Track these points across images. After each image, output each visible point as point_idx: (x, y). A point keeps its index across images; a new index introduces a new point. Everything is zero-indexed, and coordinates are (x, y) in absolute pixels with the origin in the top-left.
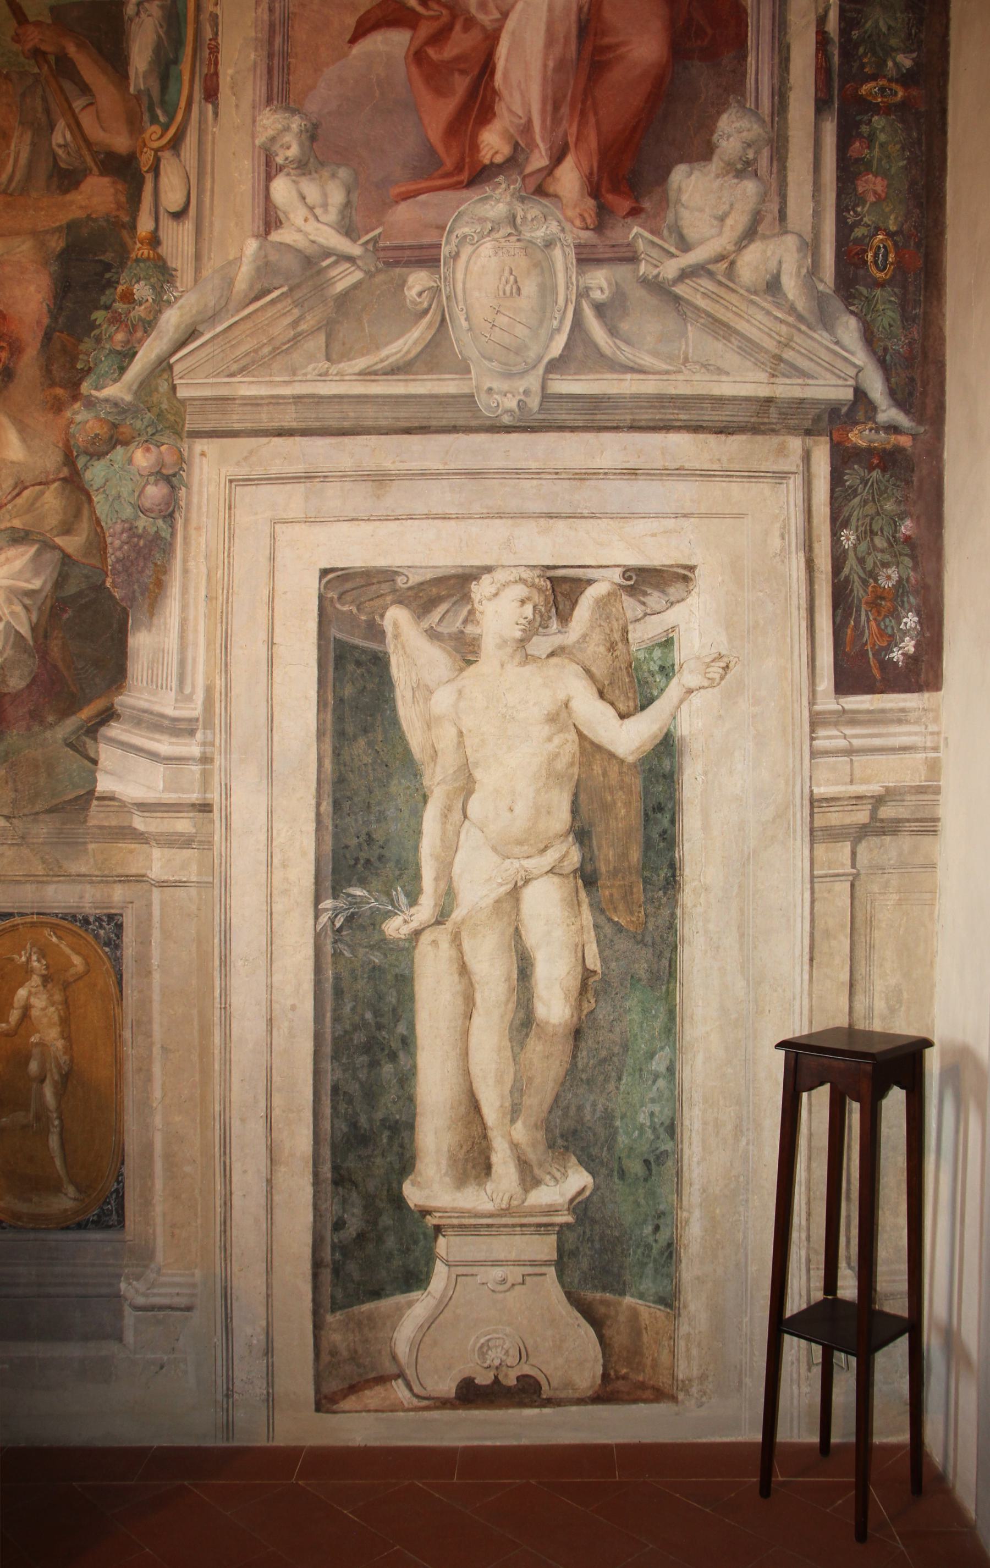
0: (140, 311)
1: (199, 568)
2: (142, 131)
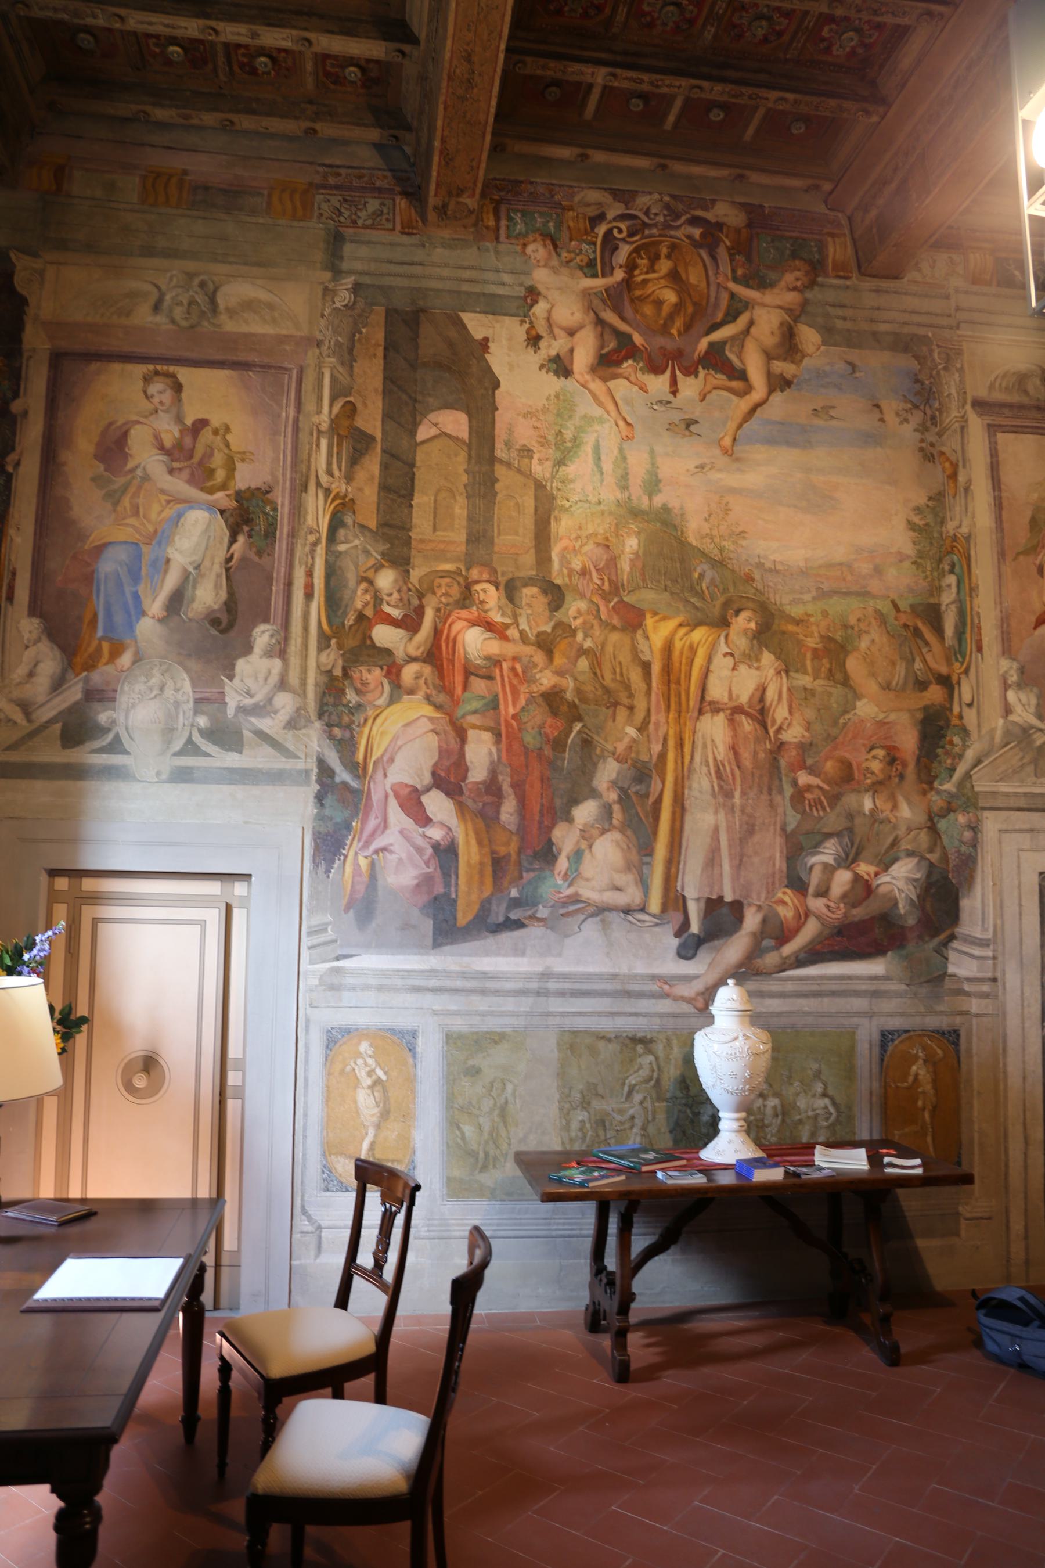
2: (952, 664)
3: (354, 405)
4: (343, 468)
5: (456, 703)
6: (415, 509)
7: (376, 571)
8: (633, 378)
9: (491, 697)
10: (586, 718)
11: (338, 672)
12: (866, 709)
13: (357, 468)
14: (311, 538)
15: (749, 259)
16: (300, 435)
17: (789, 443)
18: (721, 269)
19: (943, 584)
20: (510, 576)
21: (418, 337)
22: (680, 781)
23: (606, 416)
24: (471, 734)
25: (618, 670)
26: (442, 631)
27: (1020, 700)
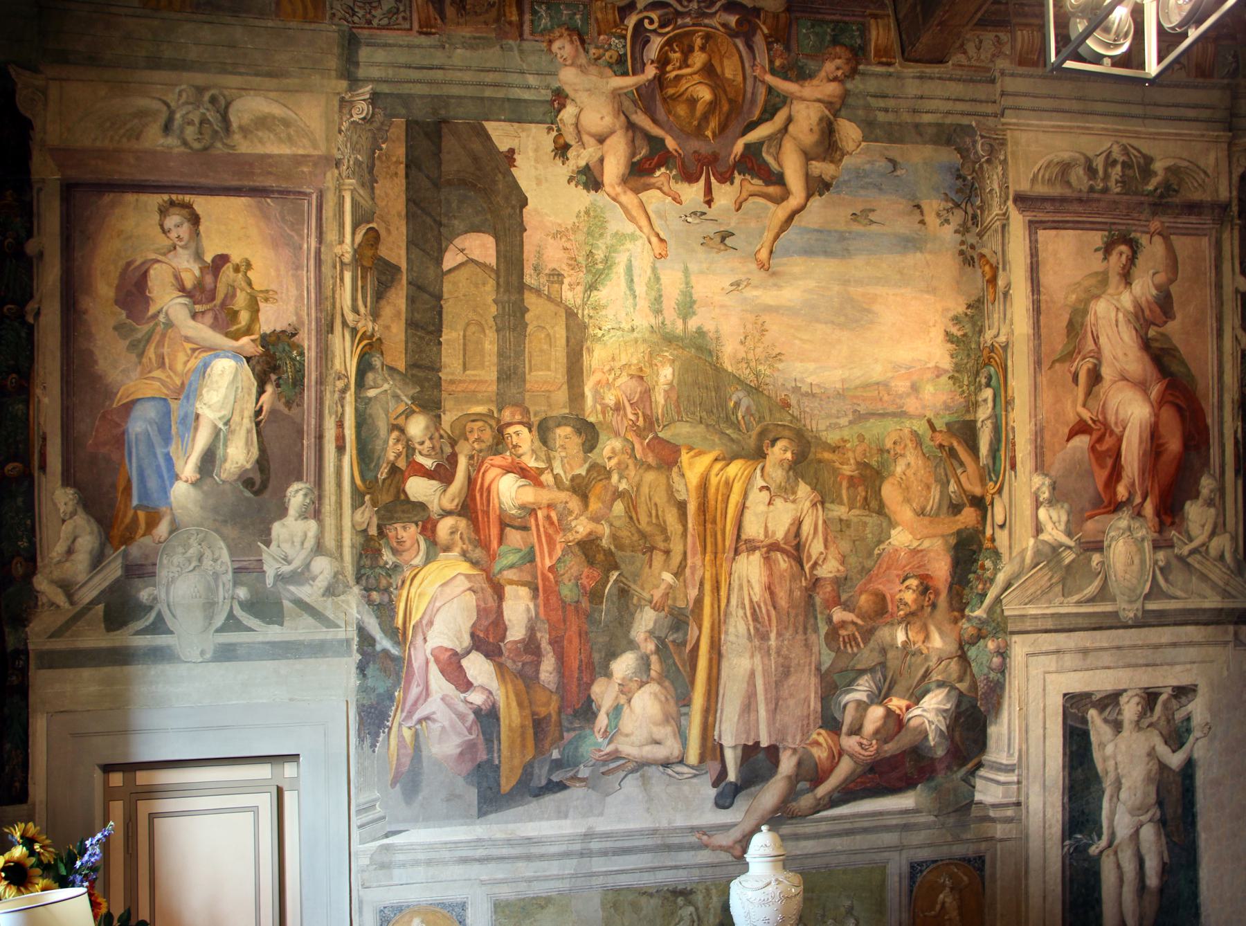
0: (988, 574)
1: (1015, 695)
2: (986, 485)
3: (377, 231)
4: (369, 304)
5: (493, 557)
6: (444, 347)
7: (407, 418)
8: (666, 189)
9: (527, 550)
10: (623, 566)
11: (373, 531)
12: (900, 538)
13: (383, 302)
14: (340, 384)
15: (788, 48)
16: (323, 269)
17: (827, 253)
18: (758, 60)
19: (980, 399)
20: (543, 416)
21: (440, 152)
22: (716, 626)
23: (638, 232)
24: (509, 589)
25: (654, 512)
26: (476, 480)
27: (1051, 518)
